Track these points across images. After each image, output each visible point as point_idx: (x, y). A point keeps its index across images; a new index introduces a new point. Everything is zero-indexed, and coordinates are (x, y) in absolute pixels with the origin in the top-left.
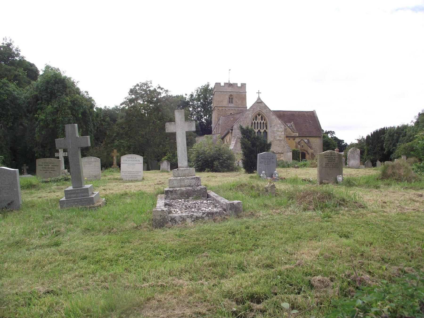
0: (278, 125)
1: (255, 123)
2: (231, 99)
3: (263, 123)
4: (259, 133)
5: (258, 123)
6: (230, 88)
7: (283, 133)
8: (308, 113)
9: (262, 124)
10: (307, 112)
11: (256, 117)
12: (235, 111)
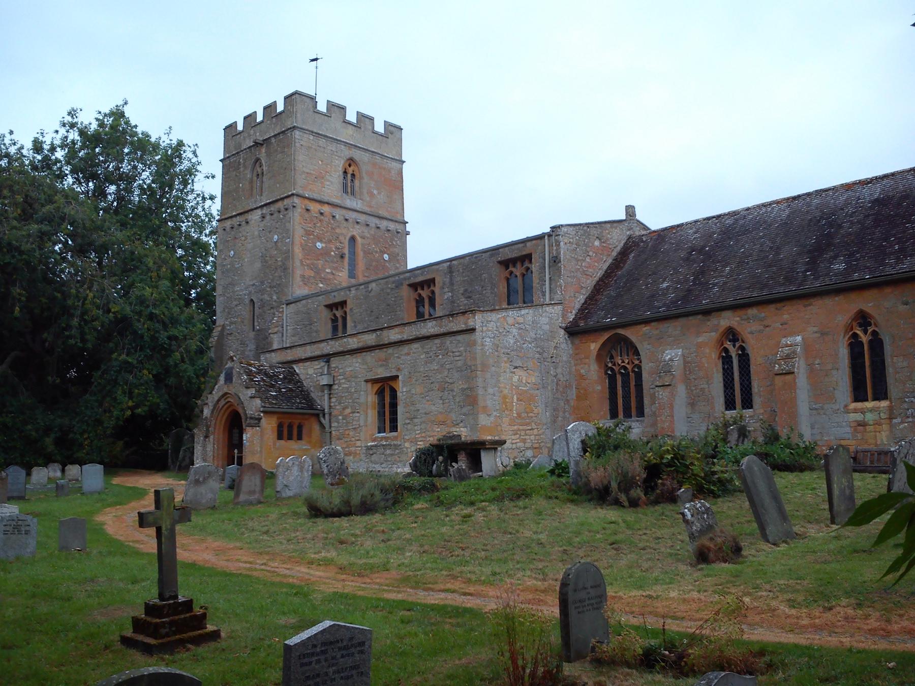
2: (349, 176)
12: (366, 230)
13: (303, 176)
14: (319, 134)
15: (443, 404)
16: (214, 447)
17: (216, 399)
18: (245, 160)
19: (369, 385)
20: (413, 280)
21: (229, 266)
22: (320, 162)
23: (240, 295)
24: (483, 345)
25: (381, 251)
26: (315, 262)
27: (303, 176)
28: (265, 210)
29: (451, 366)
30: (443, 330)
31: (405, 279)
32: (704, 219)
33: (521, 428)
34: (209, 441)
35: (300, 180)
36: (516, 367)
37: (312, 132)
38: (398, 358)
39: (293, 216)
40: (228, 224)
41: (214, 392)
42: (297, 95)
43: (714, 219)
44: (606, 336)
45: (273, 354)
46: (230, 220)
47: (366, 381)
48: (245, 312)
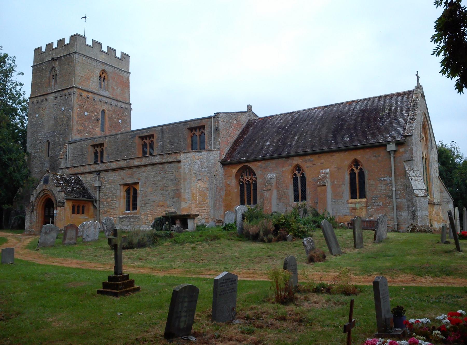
2: (102, 79)
12: (110, 107)
13: (79, 78)
14: (88, 56)
15: (163, 197)
16: (36, 217)
17: (38, 192)
18: (46, 67)
19: (122, 187)
20: (141, 135)
21: (35, 122)
22: (88, 71)
23: (41, 138)
24: (184, 169)
25: (117, 118)
26: (84, 122)
27: (79, 78)
28: (57, 94)
29: (167, 179)
30: (163, 161)
31: (137, 134)
32: (284, 114)
33: (200, 209)
34: (34, 213)
35: (78, 80)
36: (199, 180)
37: (85, 55)
38: (139, 173)
39: (73, 98)
40: (35, 100)
41: (37, 189)
42: (77, 36)
43: (289, 114)
44: (240, 166)
45: (67, 169)
46: (36, 98)
47: (120, 185)
48: (44, 147)
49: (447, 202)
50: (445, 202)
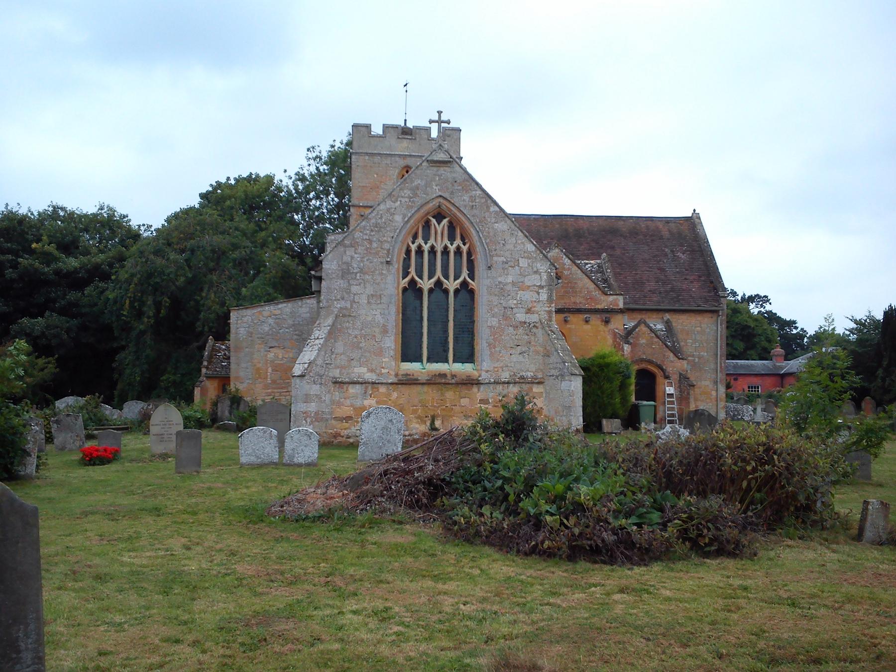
0: (523, 263)
1: (420, 251)
3: (458, 251)
4: (438, 294)
5: (432, 251)
6: (405, 143)
7: (544, 296)
8: (672, 225)
9: (452, 255)
10: (667, 221)
11: (427, 224)
13: (360, 190)
22: (375, 176)
24: (237, 333)
27: (360, 190)
33: (276, 391)
36: (272, 347)
49: (557, 377)
50: (553, 376)
